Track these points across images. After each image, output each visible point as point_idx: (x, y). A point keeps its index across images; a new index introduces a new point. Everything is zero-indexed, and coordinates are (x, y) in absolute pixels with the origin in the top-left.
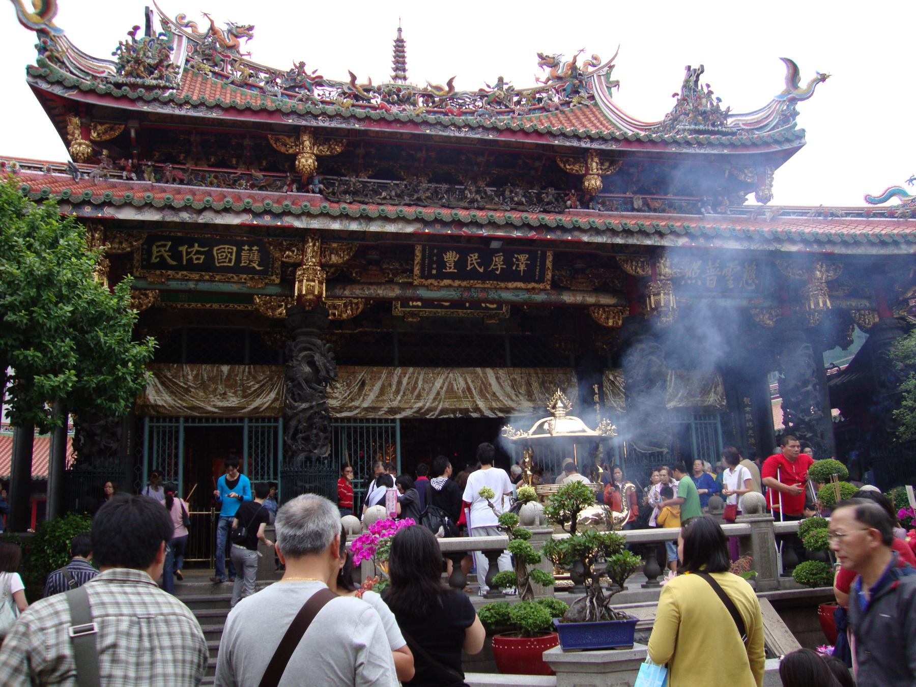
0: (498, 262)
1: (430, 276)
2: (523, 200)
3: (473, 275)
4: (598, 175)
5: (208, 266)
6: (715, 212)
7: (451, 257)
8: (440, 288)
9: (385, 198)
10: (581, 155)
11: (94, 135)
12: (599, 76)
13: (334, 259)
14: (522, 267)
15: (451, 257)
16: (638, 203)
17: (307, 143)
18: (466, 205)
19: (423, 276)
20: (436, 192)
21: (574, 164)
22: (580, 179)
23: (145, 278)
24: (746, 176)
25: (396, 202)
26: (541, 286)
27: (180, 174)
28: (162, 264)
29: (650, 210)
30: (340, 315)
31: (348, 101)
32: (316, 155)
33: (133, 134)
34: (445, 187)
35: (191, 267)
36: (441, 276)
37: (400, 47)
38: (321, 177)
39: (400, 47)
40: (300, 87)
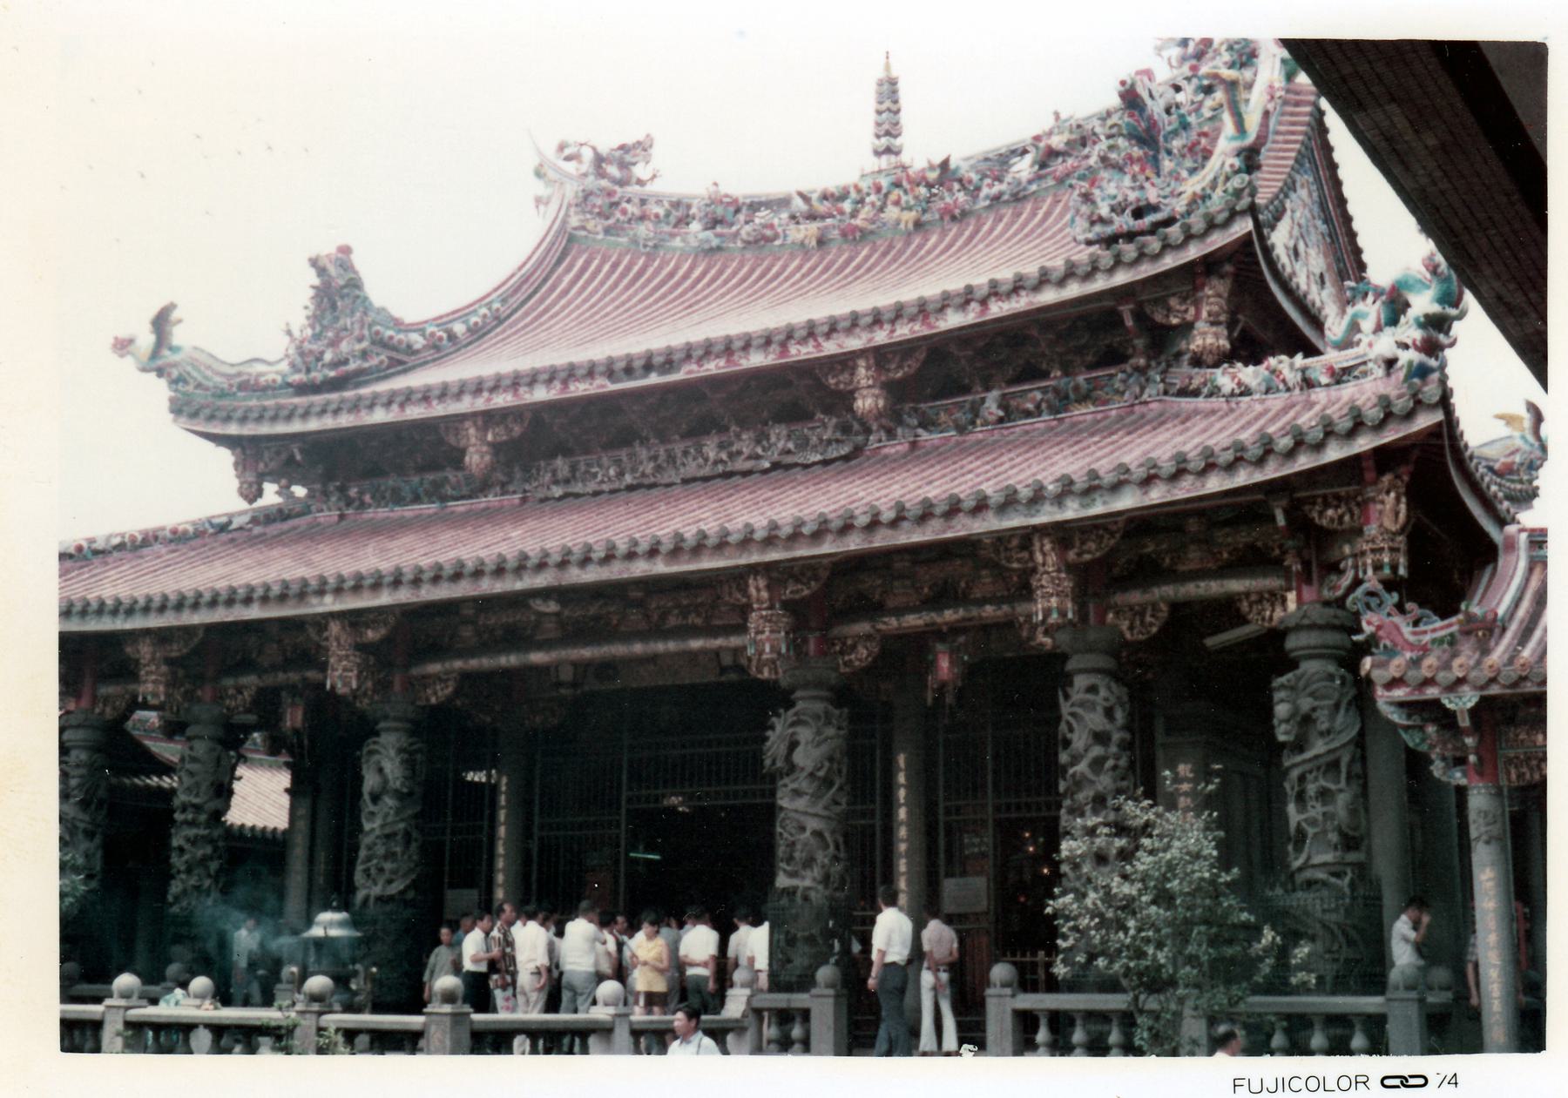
2: (791, 445)
4: (869, 387)
9: (602, 482)
10: (846, 361)
11: (261, 466)
13: (370, 635)
17: (472, 431)
18: (706, 471)
20: (669, 456)
21: (842, 371)
22: (848, 397)
24: (1169, 310)
25: (616, 485)
30: (428, 700)
32: (489, 444)
33: (298, 457)
34: (678, 448)
37: (889, 91)
39: (889, 91)
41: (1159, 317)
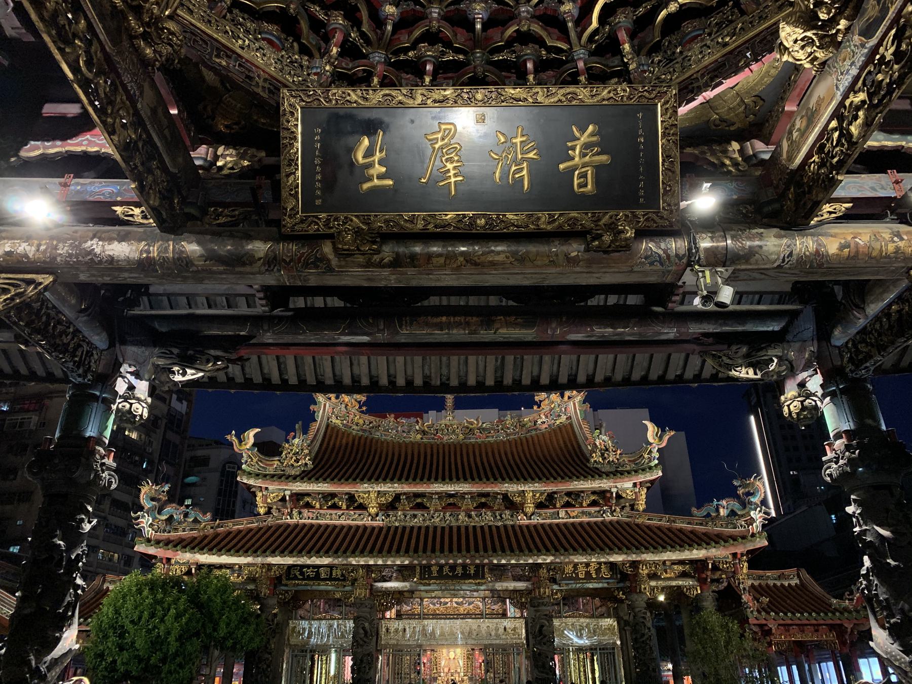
0: (459, 570)
1: (426, 579)
3: (447, 577)
5: (317, 577)
6: (613, 516)
7: (434, 569)
8: (429, 585)
12: (574, 404)
14: (472, 572)
15: (434, 569)
16: (562, 513)
19: (421, 579)
23: (286, 585)
26: (483, 581)
27: (310, 515)
28: (296, 578)
29: (570, 517)
31: (419, 436)
33: (287, 498)
35: (309, 578)
36: (431, 578)
38: (383, 512)
40: (392, 429)
41: (624, 495)
